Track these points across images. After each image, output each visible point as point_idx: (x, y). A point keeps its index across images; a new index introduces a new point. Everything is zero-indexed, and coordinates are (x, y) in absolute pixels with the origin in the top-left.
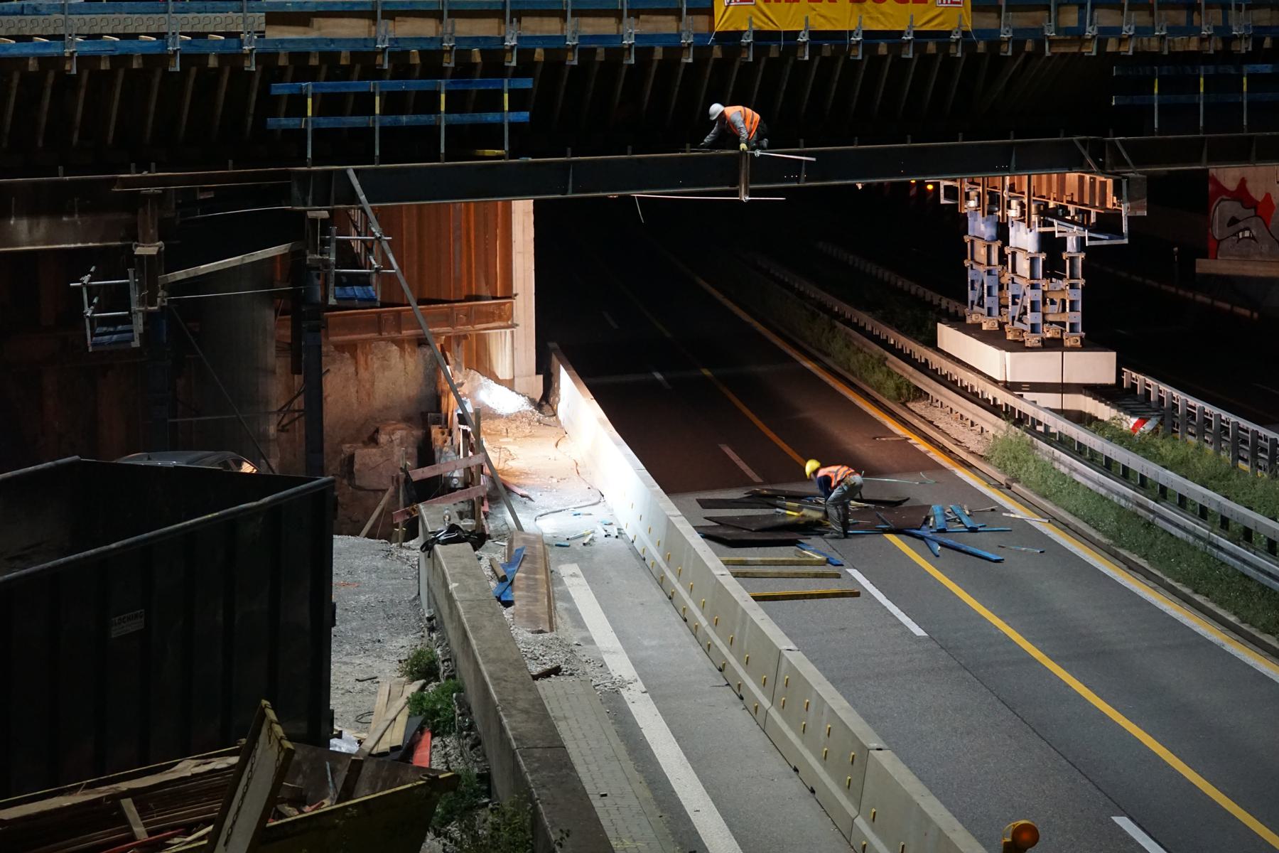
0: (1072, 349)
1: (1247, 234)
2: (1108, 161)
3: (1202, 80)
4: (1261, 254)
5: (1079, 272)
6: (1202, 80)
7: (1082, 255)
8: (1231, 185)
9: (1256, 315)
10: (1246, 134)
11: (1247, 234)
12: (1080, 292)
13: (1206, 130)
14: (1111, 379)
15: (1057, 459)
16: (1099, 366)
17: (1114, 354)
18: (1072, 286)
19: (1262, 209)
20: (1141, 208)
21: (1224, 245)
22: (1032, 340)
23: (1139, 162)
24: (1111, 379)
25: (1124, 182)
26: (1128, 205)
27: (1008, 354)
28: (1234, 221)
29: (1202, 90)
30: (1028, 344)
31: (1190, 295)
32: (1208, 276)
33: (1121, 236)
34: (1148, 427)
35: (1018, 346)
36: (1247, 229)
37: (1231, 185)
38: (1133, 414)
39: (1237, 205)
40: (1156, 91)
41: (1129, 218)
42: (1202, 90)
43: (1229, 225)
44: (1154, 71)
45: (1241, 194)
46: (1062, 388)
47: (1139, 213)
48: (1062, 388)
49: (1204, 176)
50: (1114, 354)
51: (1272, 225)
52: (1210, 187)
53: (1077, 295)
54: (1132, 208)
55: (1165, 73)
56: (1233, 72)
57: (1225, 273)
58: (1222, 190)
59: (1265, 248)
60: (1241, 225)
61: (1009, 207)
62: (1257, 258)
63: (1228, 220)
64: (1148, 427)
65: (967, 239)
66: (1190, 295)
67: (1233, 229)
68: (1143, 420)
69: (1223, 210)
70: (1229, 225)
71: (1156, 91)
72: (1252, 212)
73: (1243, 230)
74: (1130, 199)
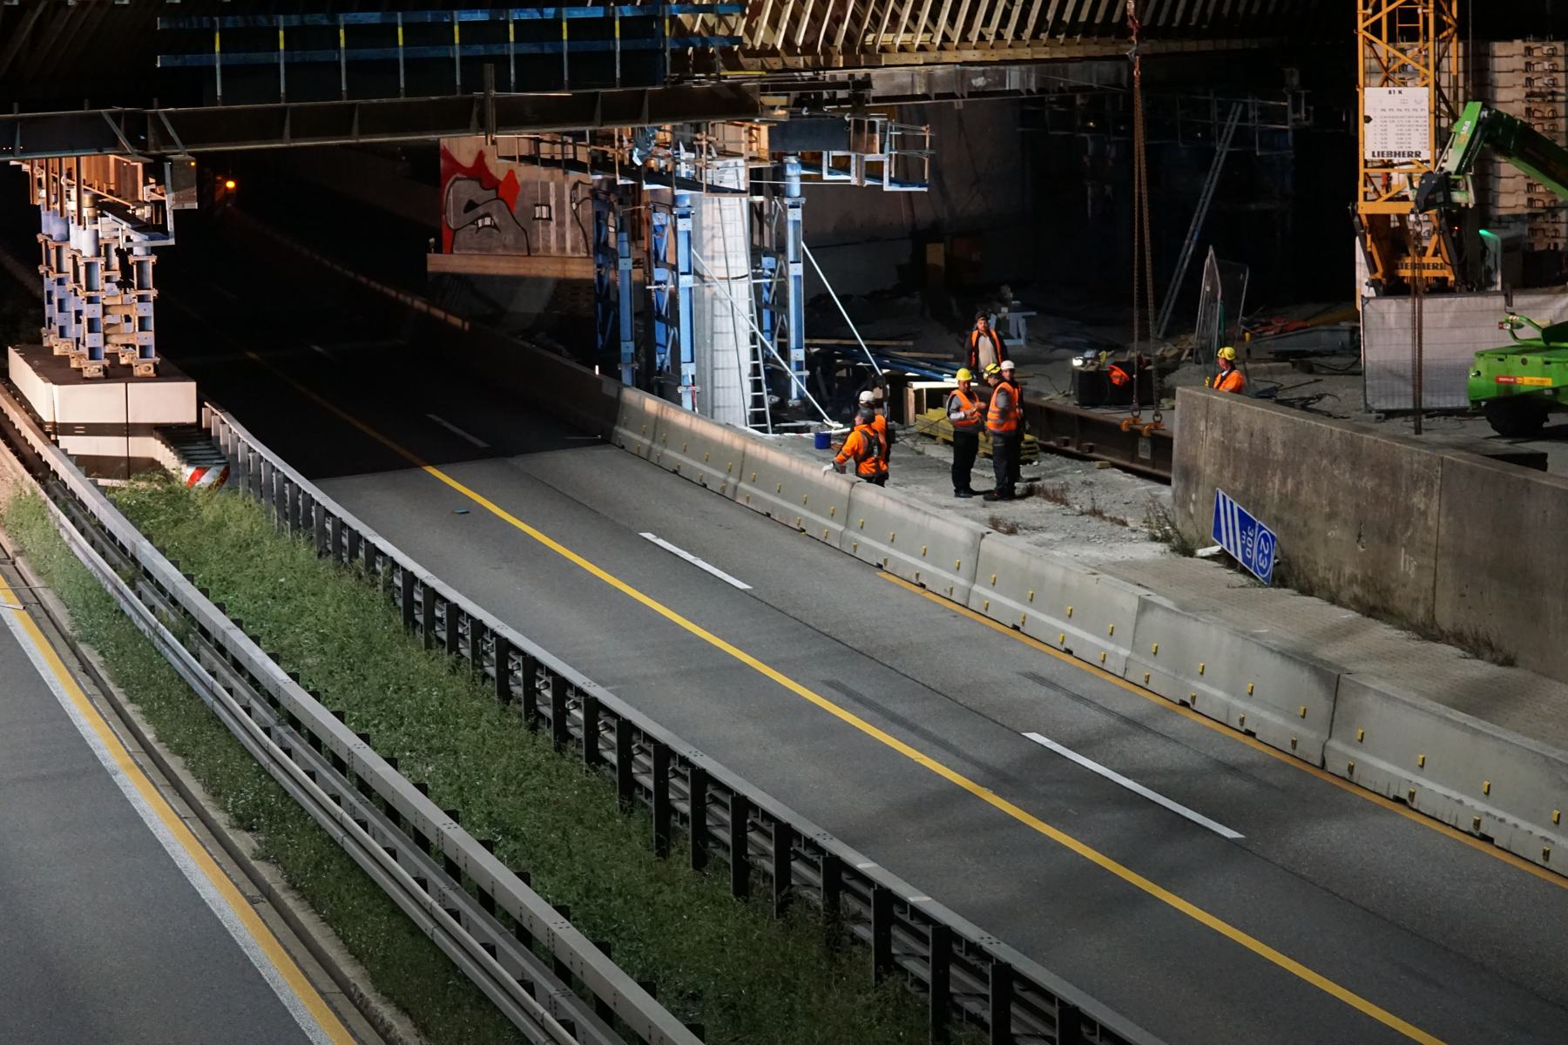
0: (145, 379)
1: (488, 221)
2: (151, 141)
3: (281, 33)
4: (505, 247)
5: (149, 279)
6: (281, 33)
7: (153, 259)
8: (467, 160)
9: (467, 326)
10: (402, 99)
11: (488, 221)
12: (151, 306)
13: (289, 98)
14: (193, 419)
15: (61, 525)
16: (175, 401)
17: (190, 387)
18: (141, 299)
19: (504, 191)
20: (189, 199)
21: (461, 236)
22: (92, 369)
23: (186, 143)
24: (193, 419)
25: (167, 165)
26: (172, 195)
27: (56, 387)
28: (471, 206)
29: (282, 46)
30: (86, 374)
31: (409, 300)
32: (442, 276)
33: (166, 235)
34: (207, 479)
35: (77, 377)
36: (488, 215)
37: (467, 160)
38: (190, 463)
39: (475, 184)
40: (217, 48)
41: (176, 212)
42: (282, 46)
43: (466, 211)
44: (214, 23)
45: (479, 171)
46: (128, 430)
47: (188, 206)
48: (128, 430)
49: (435, 151)
50: (190, 387)
51: (517, 209)
52: (442, 162)
53: (148, 310)
54: (177, 200)
55: (228, 25)
56: (325, 22)
57: (461, 270)
58: (456, 166)
59: (509, 238)
60: (481, 211)
61: (68, 196)
62: (500, 251)
63: (464, 204)
64: (207, 479)
65: (40, 238)
66: (409, 300)
67: (471, 215)
68: (202, 471)
69: (458, 191)
70: (466, 211)
71: (217, 48)
72: (493, 192)
73: (483, 217)
74: (175, 189)
